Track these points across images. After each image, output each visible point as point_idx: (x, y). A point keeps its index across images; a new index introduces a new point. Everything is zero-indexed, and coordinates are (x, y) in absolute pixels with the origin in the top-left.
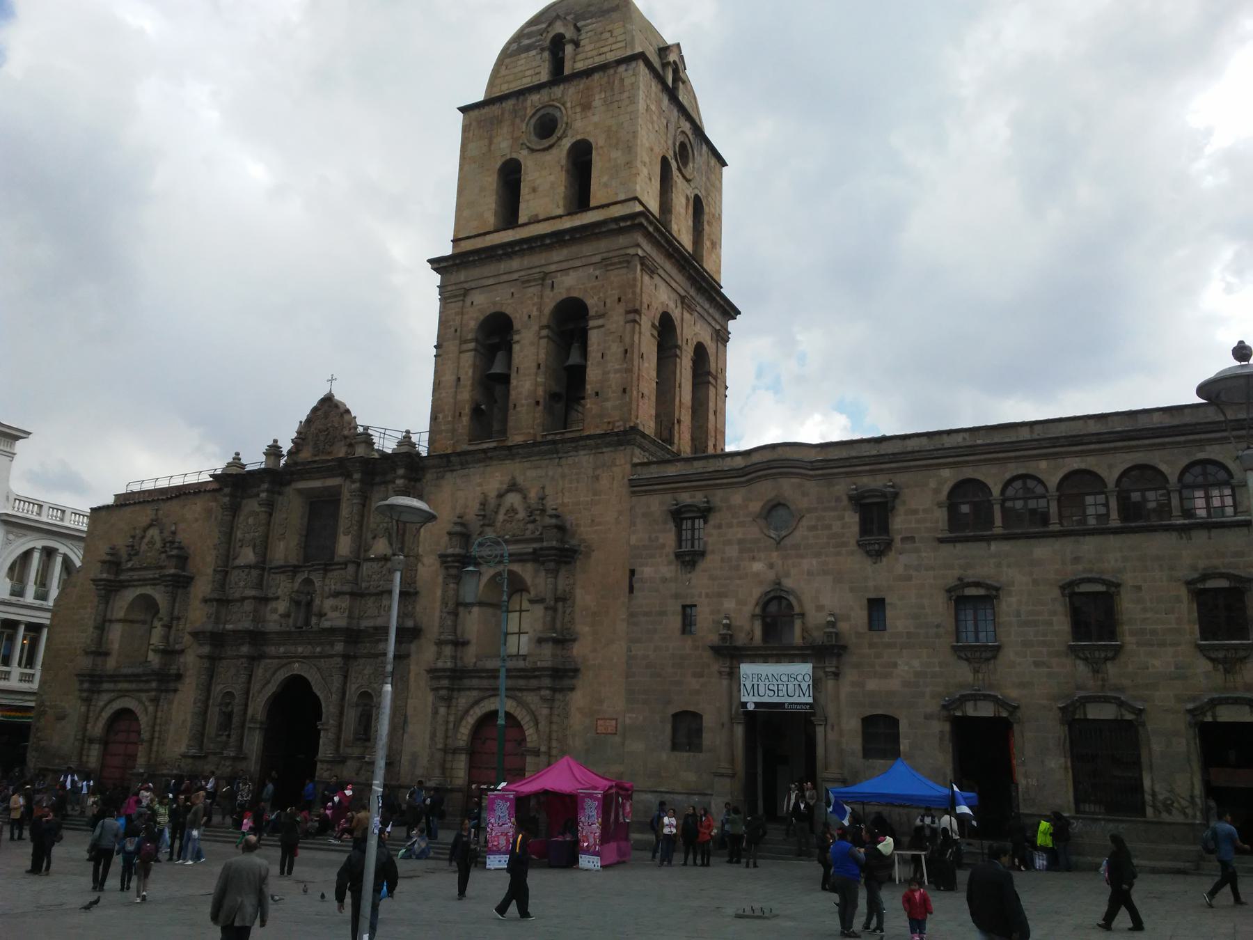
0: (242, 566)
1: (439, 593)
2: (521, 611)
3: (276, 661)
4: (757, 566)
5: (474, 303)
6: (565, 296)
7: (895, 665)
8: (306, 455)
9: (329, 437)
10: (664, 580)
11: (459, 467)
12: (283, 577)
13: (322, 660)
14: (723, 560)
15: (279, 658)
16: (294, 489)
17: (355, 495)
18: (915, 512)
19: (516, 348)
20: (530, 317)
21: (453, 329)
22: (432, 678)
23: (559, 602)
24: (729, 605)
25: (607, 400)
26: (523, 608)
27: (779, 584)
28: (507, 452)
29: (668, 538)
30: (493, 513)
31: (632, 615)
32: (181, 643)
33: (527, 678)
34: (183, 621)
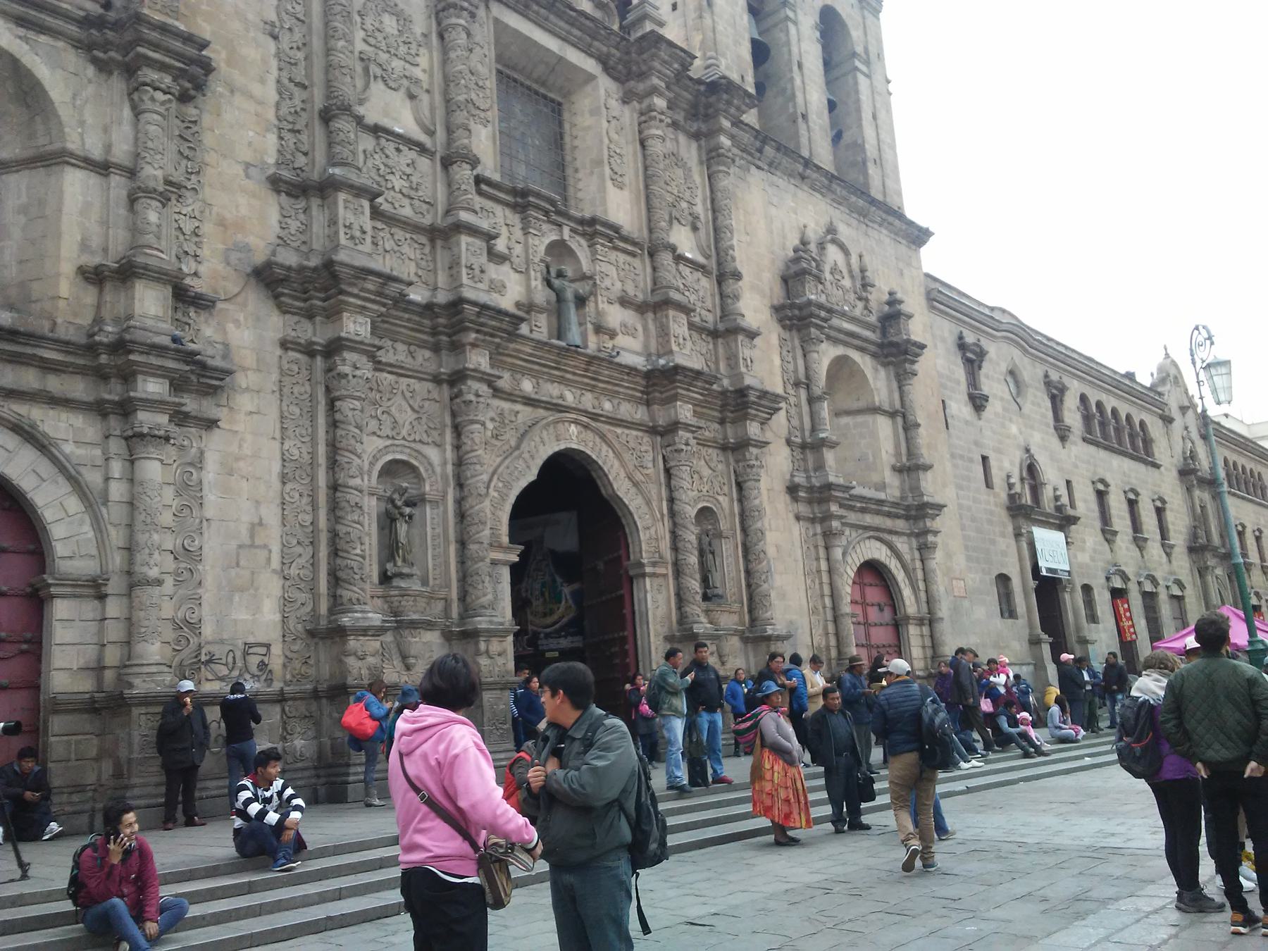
0: (399, 136)
1: (777, 361)
3: (526, 413)
7: (1084, 541)
10: (967, 422)
11: (766, 167)
12: (508, 212)
13: (619, 431)
15: (530, 402)
16: (497, 21)
17: (661, 121)
18: (1070, 410)
22: (795, 499)
23: (904, 418)
24: (1007, 465)
27: (1028, 451)
28: (826, 182)
29: (960, 373)
31: (953, 456)
33: (897, 516)
34: (191, 205)
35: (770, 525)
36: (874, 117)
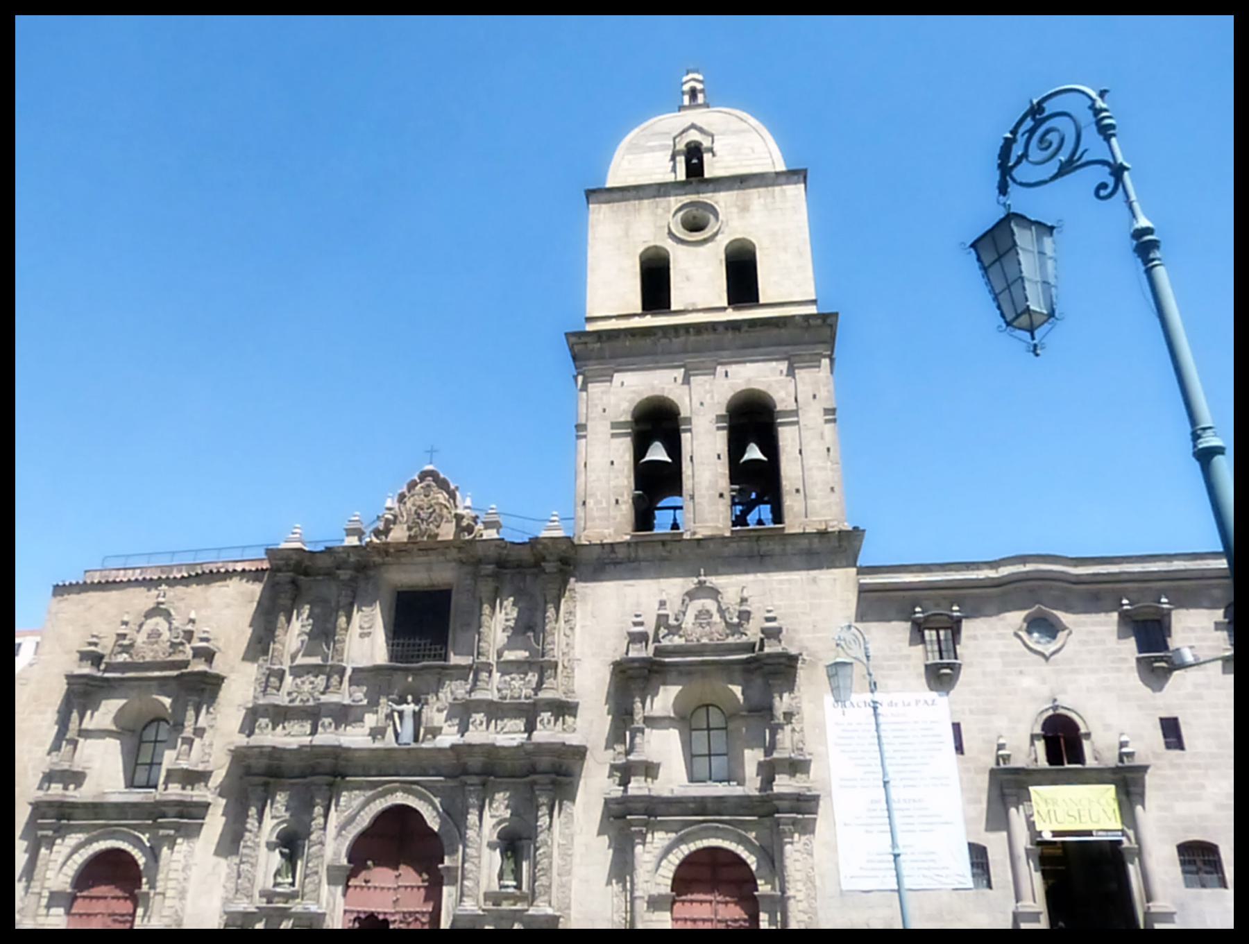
2: (709, 729)
4: (1027, 682)
5: (625, 384)
6: (744, 387)
7: (1203, 787)
8: (399, 534)
9: (434, 515)
14: (984, 674)
19: (685, 437)
20: (702, 404)
21: (600, 410)
24: (1000, 723)
25: (814, 498)
26: (711, 726)
27: (1055, 700)
30: (682, 615)
32: (208, 761)
35: (581, 830)
36: (800, 452)
